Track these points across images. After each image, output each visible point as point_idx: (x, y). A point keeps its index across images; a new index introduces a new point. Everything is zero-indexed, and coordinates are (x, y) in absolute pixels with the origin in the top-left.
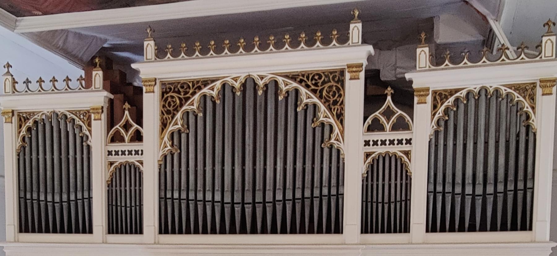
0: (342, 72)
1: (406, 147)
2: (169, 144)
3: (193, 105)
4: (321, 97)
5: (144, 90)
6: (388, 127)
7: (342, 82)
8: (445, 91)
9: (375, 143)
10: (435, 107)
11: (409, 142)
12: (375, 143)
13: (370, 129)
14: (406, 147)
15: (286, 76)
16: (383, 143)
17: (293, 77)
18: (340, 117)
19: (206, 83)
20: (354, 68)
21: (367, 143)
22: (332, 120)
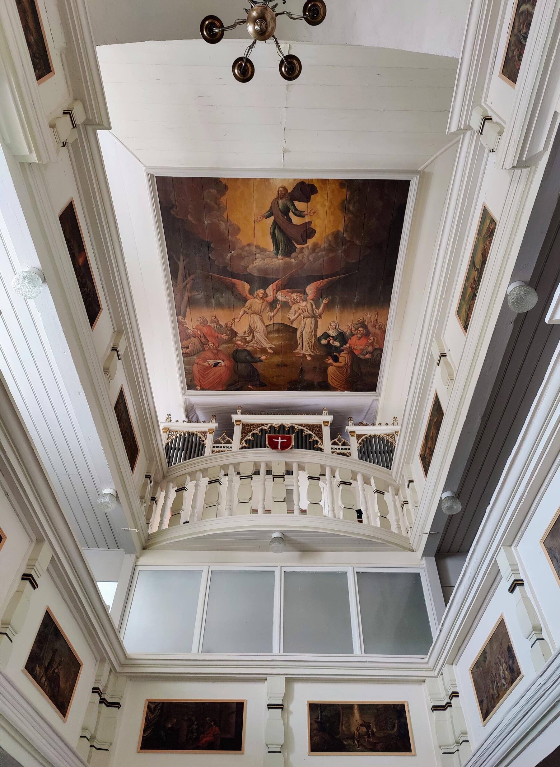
0: (321, 425)
1: (349, 451)
2: (244, 443)
3: (257, 431)
4: (312, 432)
5: (235, 424)
6: (340, 444)
7: (321, 429)
8: (361, 434)
9: (336, 449)
10: (358, 439)
11: (349, 449)
12: (336, 449)
13: (332, 444)
14: (349, 451)
15: (298, 425)
16: (339, 449)
17: (301, 425)
18: (321, 438)
19: (263, 425)
20: (326, 423)
21: (332, 449)
22: (318, 439)
